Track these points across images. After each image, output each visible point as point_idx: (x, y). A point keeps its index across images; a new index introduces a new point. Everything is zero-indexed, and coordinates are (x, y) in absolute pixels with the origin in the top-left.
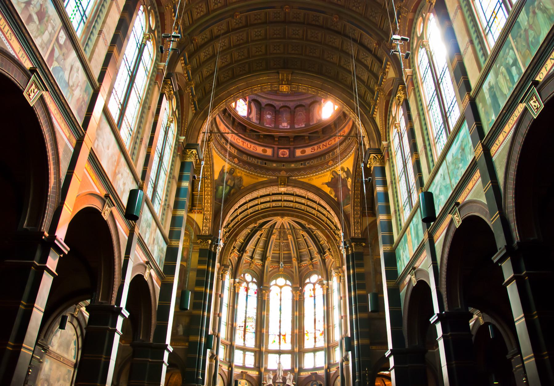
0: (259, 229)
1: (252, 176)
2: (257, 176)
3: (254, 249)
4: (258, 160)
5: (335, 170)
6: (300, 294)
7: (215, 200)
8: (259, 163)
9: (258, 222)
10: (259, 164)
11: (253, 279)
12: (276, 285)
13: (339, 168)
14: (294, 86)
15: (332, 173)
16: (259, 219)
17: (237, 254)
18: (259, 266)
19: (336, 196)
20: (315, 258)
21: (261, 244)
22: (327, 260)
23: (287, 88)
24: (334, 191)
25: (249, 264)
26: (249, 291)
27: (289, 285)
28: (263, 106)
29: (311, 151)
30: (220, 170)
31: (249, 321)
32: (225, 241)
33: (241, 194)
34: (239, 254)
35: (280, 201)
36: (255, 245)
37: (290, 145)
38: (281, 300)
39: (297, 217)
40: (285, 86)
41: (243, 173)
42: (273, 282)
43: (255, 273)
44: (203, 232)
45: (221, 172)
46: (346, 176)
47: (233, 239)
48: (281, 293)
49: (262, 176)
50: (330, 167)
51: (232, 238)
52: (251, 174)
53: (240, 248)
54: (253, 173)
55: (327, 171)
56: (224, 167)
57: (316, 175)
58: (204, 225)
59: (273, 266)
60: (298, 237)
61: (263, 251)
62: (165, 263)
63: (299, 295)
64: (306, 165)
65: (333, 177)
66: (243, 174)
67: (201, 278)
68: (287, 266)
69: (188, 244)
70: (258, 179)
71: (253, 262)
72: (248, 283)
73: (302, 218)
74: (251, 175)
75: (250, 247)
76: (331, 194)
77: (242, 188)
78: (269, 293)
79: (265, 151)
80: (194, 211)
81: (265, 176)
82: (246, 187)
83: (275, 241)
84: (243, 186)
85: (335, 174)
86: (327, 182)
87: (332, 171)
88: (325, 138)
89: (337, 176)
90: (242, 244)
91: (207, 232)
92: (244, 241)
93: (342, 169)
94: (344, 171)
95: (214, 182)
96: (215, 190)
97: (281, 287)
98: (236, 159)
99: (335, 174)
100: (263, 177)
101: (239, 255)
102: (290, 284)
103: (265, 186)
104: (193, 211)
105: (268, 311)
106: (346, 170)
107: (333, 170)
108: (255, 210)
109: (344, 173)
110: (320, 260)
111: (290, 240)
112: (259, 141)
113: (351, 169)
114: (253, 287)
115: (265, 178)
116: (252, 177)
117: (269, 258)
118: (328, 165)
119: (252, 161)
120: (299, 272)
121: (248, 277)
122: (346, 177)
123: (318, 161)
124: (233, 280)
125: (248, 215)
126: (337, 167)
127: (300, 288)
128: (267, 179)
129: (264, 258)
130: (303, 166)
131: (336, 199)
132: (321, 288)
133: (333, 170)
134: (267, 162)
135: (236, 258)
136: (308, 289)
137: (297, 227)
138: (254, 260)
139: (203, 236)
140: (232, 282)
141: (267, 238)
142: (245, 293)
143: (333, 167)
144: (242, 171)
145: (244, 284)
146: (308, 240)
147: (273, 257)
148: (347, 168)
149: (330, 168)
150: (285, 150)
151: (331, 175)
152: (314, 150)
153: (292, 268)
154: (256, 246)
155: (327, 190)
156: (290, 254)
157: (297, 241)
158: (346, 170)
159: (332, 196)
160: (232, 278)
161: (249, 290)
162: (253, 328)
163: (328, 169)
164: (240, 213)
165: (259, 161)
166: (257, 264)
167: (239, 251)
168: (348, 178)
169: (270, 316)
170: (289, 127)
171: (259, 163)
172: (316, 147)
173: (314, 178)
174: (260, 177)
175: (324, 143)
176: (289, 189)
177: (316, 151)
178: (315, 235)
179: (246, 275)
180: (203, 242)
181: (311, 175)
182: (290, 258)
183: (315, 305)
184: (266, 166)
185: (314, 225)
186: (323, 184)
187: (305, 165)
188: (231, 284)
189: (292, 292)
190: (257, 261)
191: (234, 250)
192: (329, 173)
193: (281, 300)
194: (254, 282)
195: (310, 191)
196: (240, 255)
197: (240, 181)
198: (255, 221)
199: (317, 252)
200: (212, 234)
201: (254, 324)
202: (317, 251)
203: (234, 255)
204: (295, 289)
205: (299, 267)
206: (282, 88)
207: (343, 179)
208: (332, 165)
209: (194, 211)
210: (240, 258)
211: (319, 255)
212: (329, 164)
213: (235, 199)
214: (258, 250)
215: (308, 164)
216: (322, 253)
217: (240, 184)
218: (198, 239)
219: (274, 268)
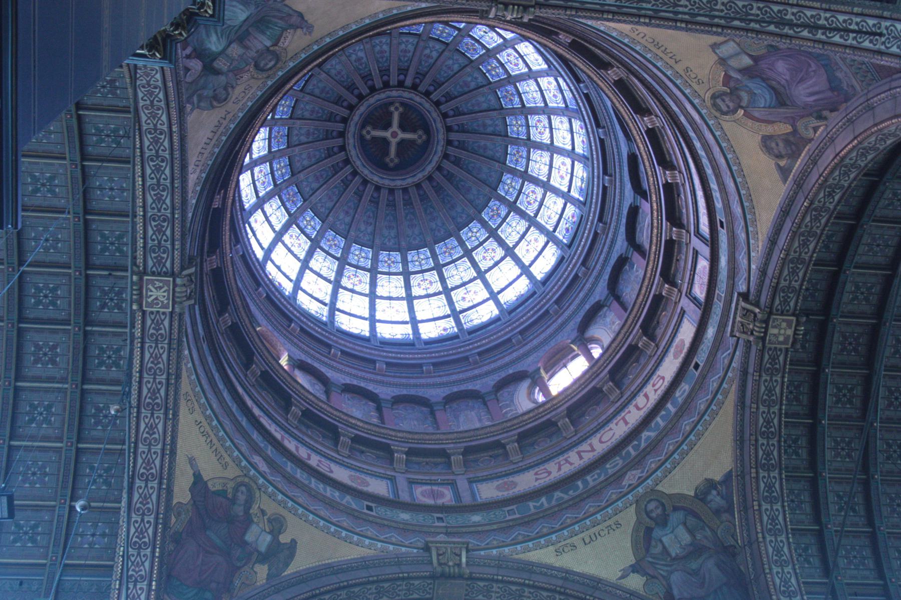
5: (257, 495)
13: (271, 508)
15: (242, 484)
23: (781, 339)
40: (790, 332)
46: (263, 548)
56: (310, 28)
65: (230, 496)
85: (242, 498)
86: (205, 479)
87: (246, 480)
89: (239, 510)
93: (277, 525)
99: (242, 498)
106: (284, 539)
109: (269, 538)
113: (301, 563)
122: (260, 553)
133: (255, 487)
148: (294, 542)
149: (253, 472)
151: (231, 485)
158: (284, 539)
168: (264, 558)
176: (158, 325)
192: (232, 472)
197: (215, 98)
206: (784, 325)
207: (246, 543)
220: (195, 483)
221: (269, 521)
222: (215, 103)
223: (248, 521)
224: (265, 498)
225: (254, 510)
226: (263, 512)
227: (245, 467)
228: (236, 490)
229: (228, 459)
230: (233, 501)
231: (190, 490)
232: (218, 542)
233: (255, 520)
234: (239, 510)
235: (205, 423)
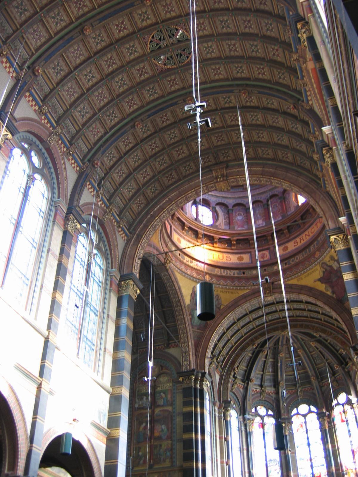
0: (261, 349)
1: (231, 291)
2: (237, 289)
3: (262, 375)
4: (234, 271)
5: (324, 261)
6: (329, 420)
7: (193, 328)
8: (236, 273)
9: (256, 342)
10: (236, 275)
11: (267, 411)
12: (298, 414)
13: (327, 259)
14: (232, 180)
15: (322, 266)
16: (257, 338)
17: (241, 385)
18: (272, 394)
19: (333, 292)
20: (337, 372)
21: (269, 368)
22: (351, 372)
23: (225, 185)
24: (330, 286)
25: (259, 394)
26: (265, 427)
27: (313, 412)
28: (230, 207)
29: (294, 246)
30: (191, 292)
31: (271, 464)
32: (221, 373)
33: (222, 315)
34: (243, 384)
35: (276, 311)
36: (261, 370)
37: (269, 245)
38: (307, 432)
39: (301, 326)
40: (221, 183)
41: (219, 290)
42: (294, 411)
43: (269, 405)
44: (184, 368)
45: (193, 295)
47: (230, 369)
48: (305, 423)
49: (242, 288)
50: (318, 259)
51: (229, 367)
52: (229, 289)
53: (244, 377)
54: (231, 288)
55: (316, 265)
57: (304, 273)
58: (184, 359)
59: (290, 391)
60: (311, 350)
61: (274, 376)
62: (109, 415)
63: (328, 422)
64: (290, 264)
65: (324, 270)
66: (219, 292)
67: (187, 423)
68: (306, 389)
69: (171, 385)
70: (238, 292)
71: (263, 391)
72: (262, 417)
73: (307, 327)
74: (229, 290)
75: (255, 374)
76: (328, 291)
77: (222, 308)
78: (291, 425)
79: (240, 259)
80: (172, 345)
81: (246, 288)
82: (227, 305)
83: (283, 361)
84: (222, 305)
86: (319, 277)
88: (306, 227)
89: (328, 269)
90: (246, 371)
91: (188, 367)
92: (247, 367)
94: (335, 260)
95: (186, 308)
96: (191, 317)
97: (305, 416)
98: (207, 276)
99: (325, 266)
100: (244, 289)
101: (244, 386)
102: (315, 410)
103: (248, 299)
104: (170, 346)
105: (293, 448)
107: (322, 262)
108: (250, 329)
110: (343, 374)
111: (301, 355)
112: (232, 249)
114: (270, 422)
115: (247, 289)
116: (230, 293)
117: (282, 382)
118: (314, 258)
119: (227, 274)
120: (323, 394)
121: (262, 410)
123: (303, 255)
124: (241, 417)
125: (242, 336)
126: (325, 257)
127: (327, 413)
128: (248, 291)
129: (276, 384)
130: (287, 266)
131: (334, 296)
132: (351, 408)
134: (245, 271)
135: (242, 390)
136: (337, 412)
137: (306, 338)
138: (265, 387)
139: (185, 372)
140: (241, 420)
141: (274, 358)
142: (262, 429)
143: (321, 259)
144: (218, 288)
145: (258, 419)
146: (323, 351)
147: (287, 381)
149: (319, 261)
150: (264, 252)
151: (322, 268)
152: (297, 244)
153: (313, 389)
154: (263, 371)
155: (322, 287)
156: (307, 372)
157: (312, 355)
159: (329, 293)
160: (240, 415)
161: (265, 426)
162: (278, 473)
163: (316, 263)
164: (232, 337)
165: (236, 271)
166: (269, 392)
167: (243, 381)
169: (297, 455)
170: (264, 224)
171: (236, 273)
172: (298, 239)
173: (303, 276)
174: (240, 289)
175: (307, 233)
177: (299, 244)
178: (329, 343)
179: (259, 408)
180: (186, 380)
181: (299, 274)
182: (307, 377)
183: (349, 431)
184: (245, 275)
185: (324, 331)
186: (315, 281)
187: (289, 263)
188: (241, 422)
189: (318, 419)
190: (269, 389)
191: (236, 381)
192: (318, 267)
193: (307, 432)
194: (269, 416)
195: (301, 294)
196: (246, 385)
198: (252, 342)
199: (337, 364)
200: (195, 367)
201: (278, 468)
202: (337, 363)
203: (238, 387)
204: (320, 416)
205: (321, 387)
206: (220, 186)
208: (320, 257)
209: (172, 345)
210: (246, 389)
211: (340, 368)
212: (316, 256)
213: (215, 322)
214: (267, 375)
215: (293, 261)
216: (343, 364)
217: (219, 304)
218: (180, 377)
219: (291, 393)
220: (321, 281)
221: (332, 260)
222: (219, 298)
223: (331, 267)
224: (325, 259)
225: (329, 263)
226: (329, 261)
227: (317, 263)
228: (323, 268)
229: (315, 268)
230: (326, 270)
231: (322, 283)
232: (335, 279)
233: (331, 264)
234: (328, 269)
235: (305, 274)
